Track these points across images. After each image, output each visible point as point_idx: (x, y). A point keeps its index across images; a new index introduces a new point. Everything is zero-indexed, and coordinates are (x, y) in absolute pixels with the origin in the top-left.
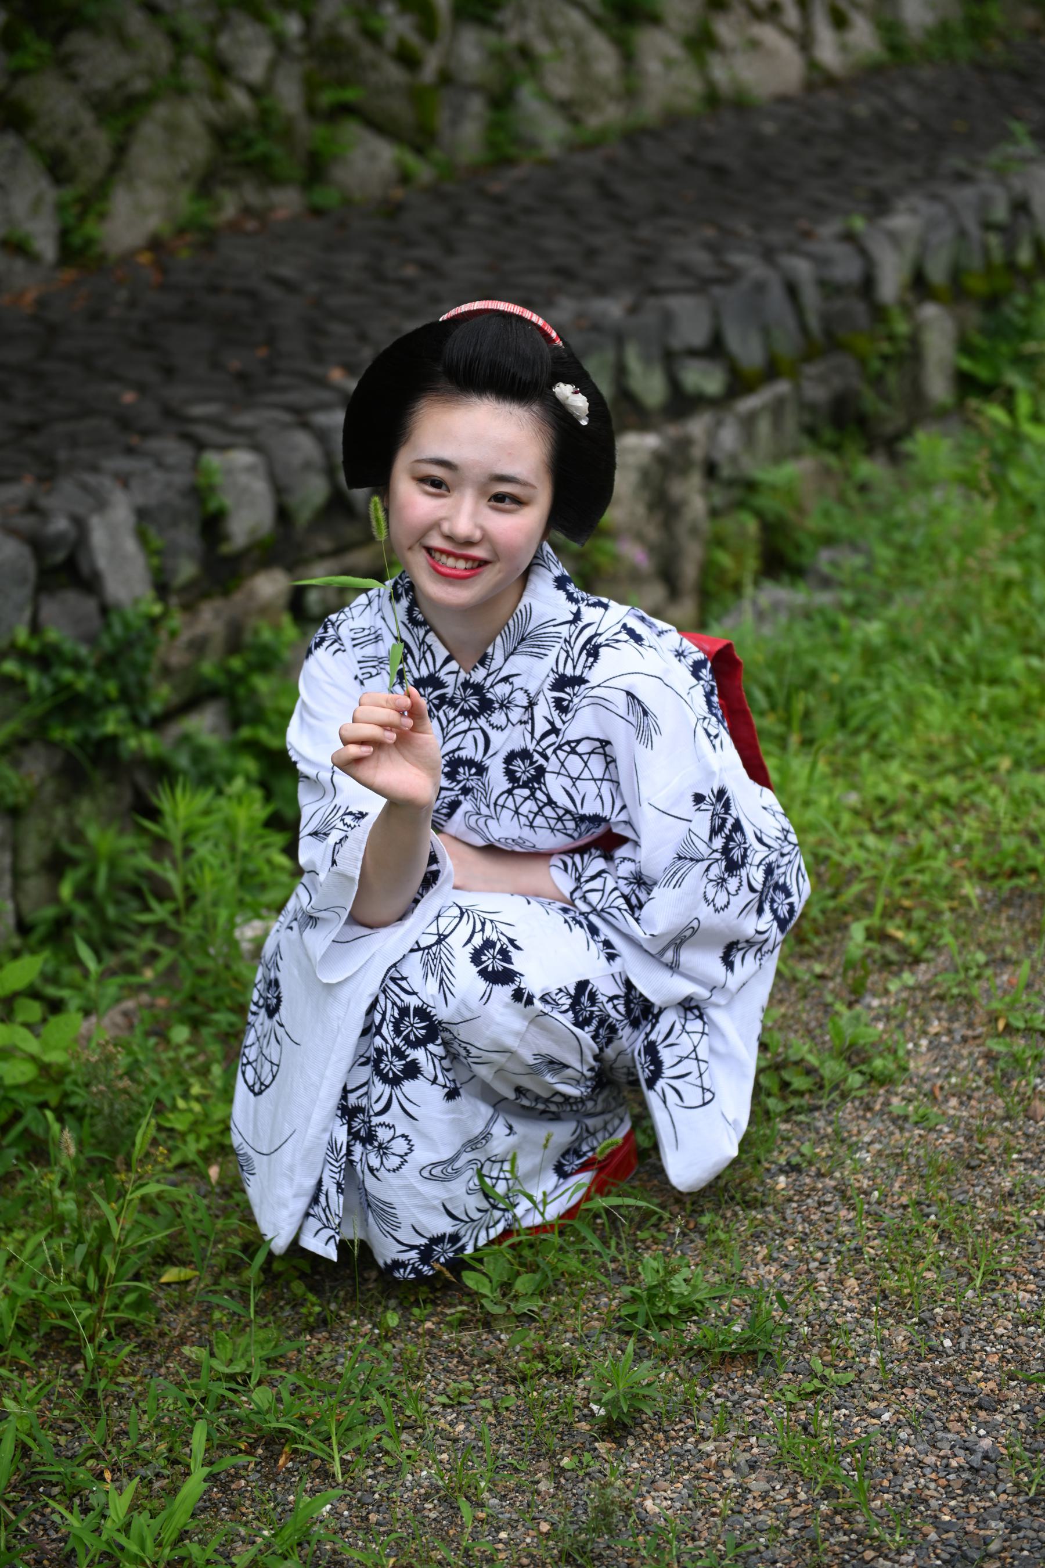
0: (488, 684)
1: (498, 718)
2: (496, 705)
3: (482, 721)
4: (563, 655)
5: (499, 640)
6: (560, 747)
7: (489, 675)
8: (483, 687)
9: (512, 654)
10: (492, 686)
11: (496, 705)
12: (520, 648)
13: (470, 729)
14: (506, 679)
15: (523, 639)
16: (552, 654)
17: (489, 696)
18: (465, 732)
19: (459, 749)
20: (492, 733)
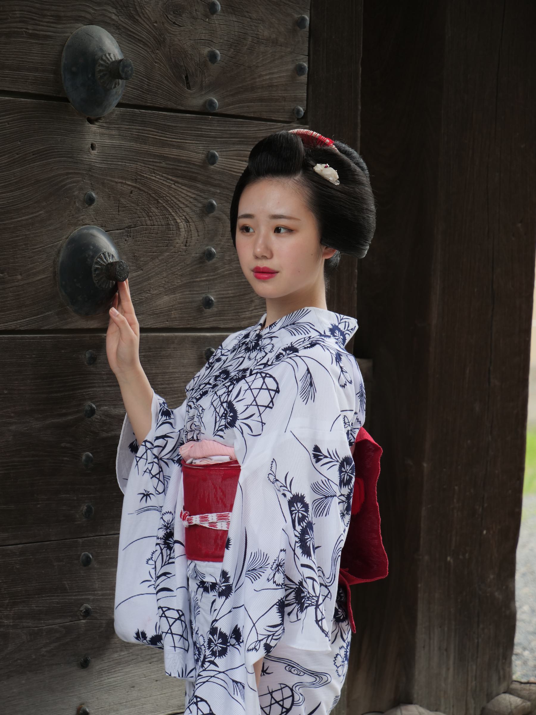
0: (264, 337)
1: (253, 354)
2: (258, 348)
3: (248, 354)
4: (303, 340)
5: (284, 318)
6: (261, 373)
7: (268, 333)
8: (262, 337)
9: (284, 327)
10: (264, 339)
11: (258, 348)
12: (289, 327)
13: (242, 357)
14: (271, 338)
15: (294, 324)
16: (298, 337)
17: (260, 342)
18: (238, 358)
19: (231, 365)
20: (246, 360)
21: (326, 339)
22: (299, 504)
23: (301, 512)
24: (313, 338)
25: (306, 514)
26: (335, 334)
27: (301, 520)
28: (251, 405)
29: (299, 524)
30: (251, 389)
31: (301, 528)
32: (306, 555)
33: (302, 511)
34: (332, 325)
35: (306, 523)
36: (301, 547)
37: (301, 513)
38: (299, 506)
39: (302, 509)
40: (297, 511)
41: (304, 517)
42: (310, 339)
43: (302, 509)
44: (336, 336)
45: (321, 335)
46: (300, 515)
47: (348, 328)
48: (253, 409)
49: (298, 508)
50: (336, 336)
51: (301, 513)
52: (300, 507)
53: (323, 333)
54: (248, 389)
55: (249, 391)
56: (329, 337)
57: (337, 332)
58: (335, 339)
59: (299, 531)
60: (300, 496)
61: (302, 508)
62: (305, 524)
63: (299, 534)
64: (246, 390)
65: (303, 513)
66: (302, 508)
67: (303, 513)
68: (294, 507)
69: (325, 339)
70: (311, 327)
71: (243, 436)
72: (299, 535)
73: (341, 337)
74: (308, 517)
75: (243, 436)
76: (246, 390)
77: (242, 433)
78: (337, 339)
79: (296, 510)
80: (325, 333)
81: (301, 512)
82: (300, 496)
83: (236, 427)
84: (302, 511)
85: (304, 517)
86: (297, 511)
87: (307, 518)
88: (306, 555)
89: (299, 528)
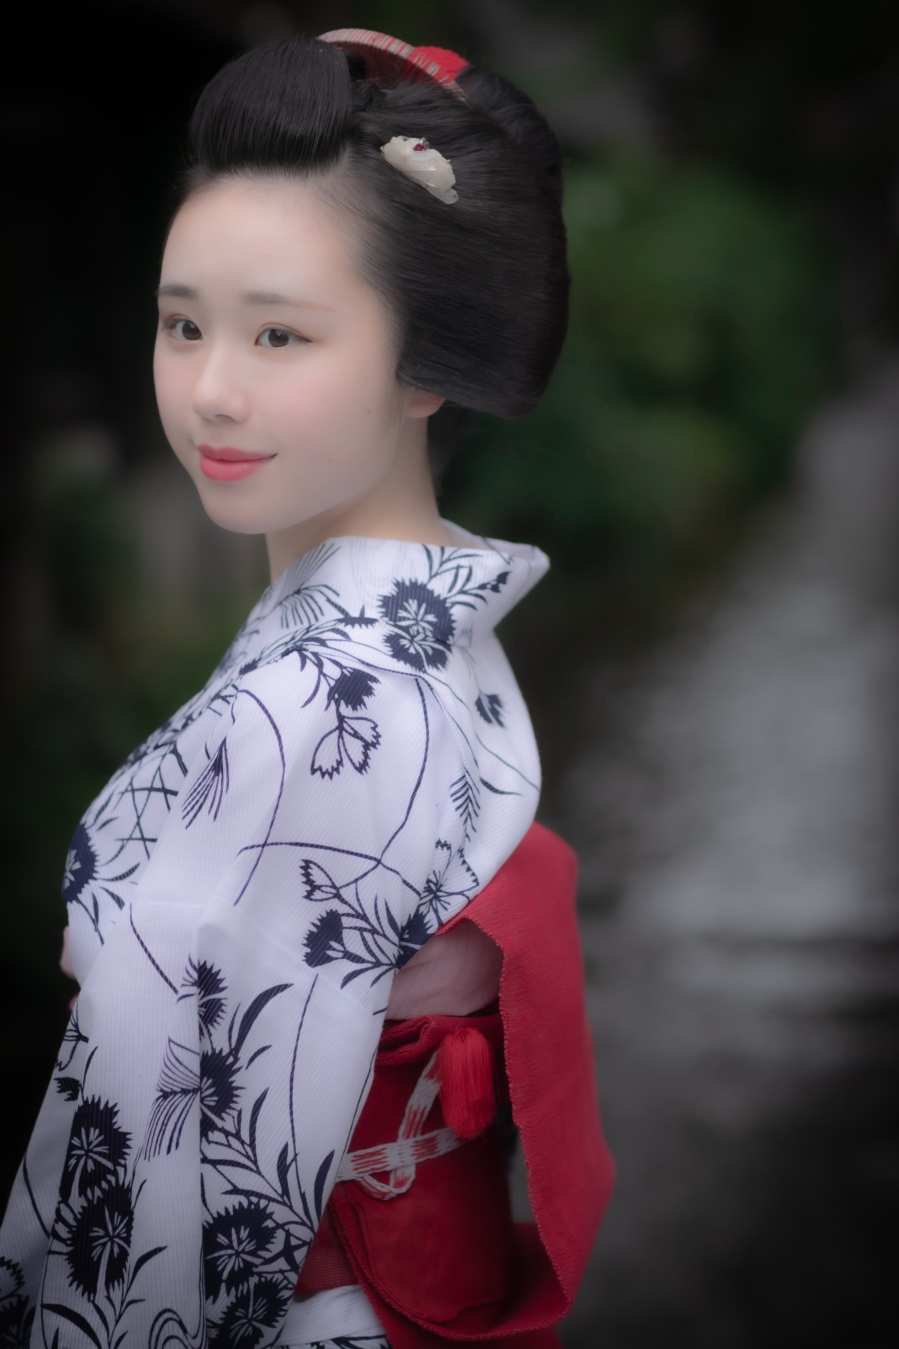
21: (355, 632)
22: (94, 1133)
23: (95, 1157)
24: (317, 628)
25: (110, 1165)
26: (402, 613)
27: (90, 1180)
28: (130, 839)
29: (82, 1192)
30: (133, 791)
31: (85, 1204)
32: (82, 1287)
33: (100, 1154)
34: (398, 584)
35: (103, 1190)
36: (71, 1258)
37: (95, 1162)
38: (92, 1137)
39: (99, 1149)
40: (82, 1152)
41: (101, 1172)
42: (308, 632)
43: (99, 1149)
44: (404, 619)
45: (348, 620)
46: (91, 1166)
47: (464, 586)
48: (135, 849)
49: (89, 1144)
50: (404, 619)
51: (95, 1162)
52: (96, 1142)
53: (355, 614)
54: (126, 791)
55: (129, 795)
56: (371, 621)
57: (413, 605)
58: (396, 626)
59: (78, 1209)
60: (102, 1106)
61: (99, 1145)
62: (98, 1192)
63: (75, 1218)
64: (123, 793)
65: (100, 1159)
66: (99, 1145)
67: (100, 1159)
68: (80, 1138)
69: (348, 629)
70: (329, 600)
71: (97, 930)
72: (73, 1223)
73: (431, 618)
74: (115, 1174)
75: (97, 930)
76: (123, 793)
77: (95, 921)
78: (406, 629)
79: (82, 1148)
80: (362, 612)
81: (95, 1157)
82: (102, 1106)
83: (79, 902)
84: (100, 1154)
85: (101, 1172)
86: (82, 1152)
87: (110, 1178)
88: (82, 1287)
89: (77, 1201)
